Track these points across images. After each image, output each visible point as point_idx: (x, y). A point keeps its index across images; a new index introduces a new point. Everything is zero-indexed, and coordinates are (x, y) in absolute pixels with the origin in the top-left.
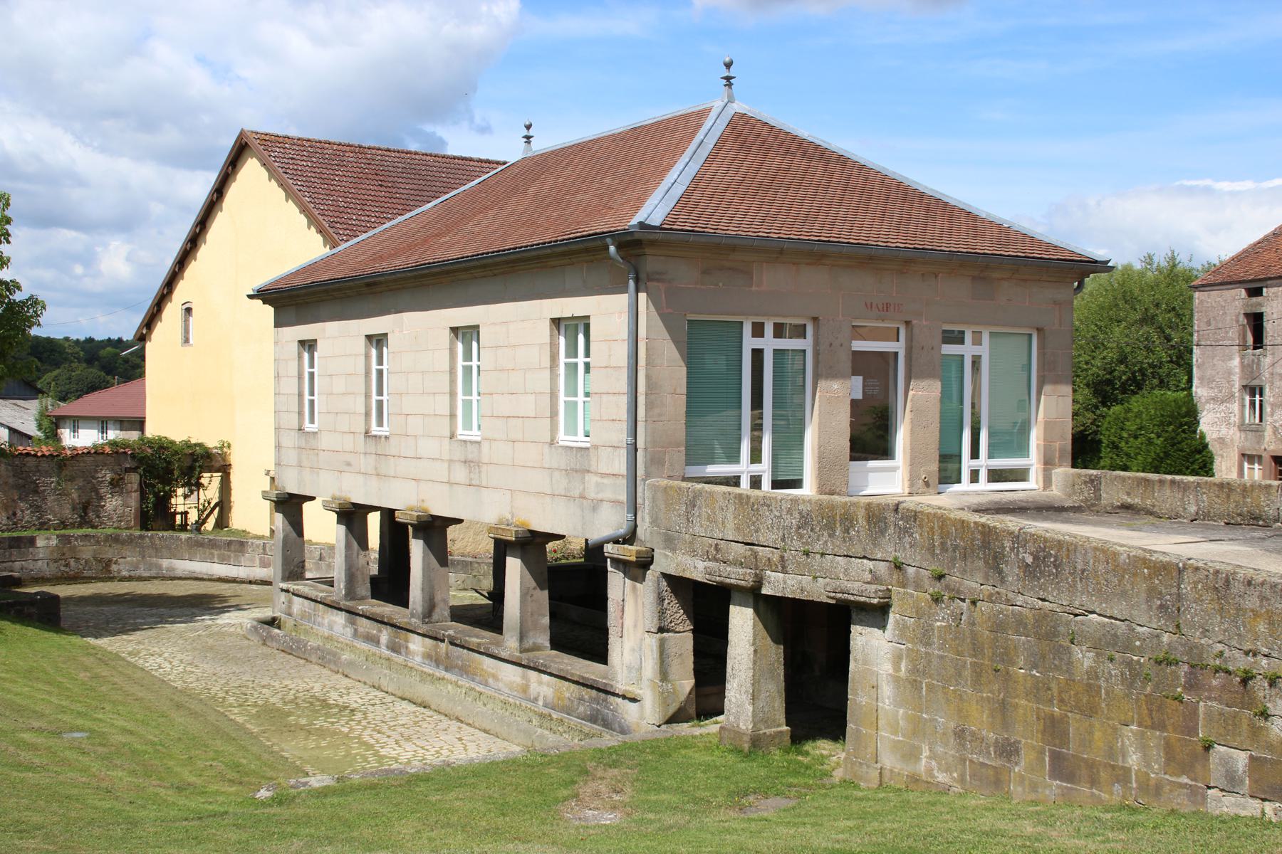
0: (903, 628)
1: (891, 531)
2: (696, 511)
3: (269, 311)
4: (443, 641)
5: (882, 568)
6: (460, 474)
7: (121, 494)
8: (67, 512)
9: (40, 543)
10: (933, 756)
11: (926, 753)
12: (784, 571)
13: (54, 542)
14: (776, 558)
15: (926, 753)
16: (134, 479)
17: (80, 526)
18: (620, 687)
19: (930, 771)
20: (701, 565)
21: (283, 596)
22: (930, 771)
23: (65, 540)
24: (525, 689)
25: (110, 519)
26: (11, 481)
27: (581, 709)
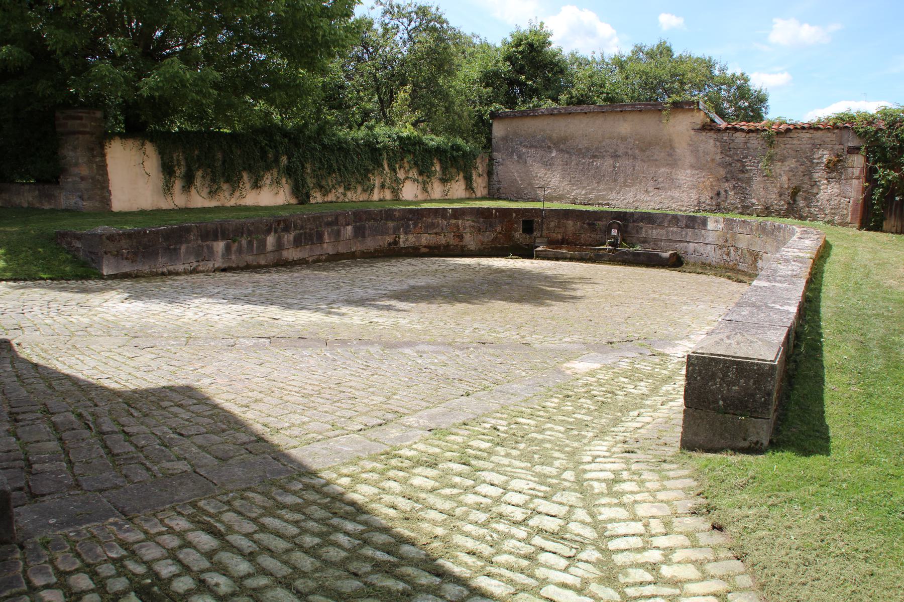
7: (839, 181)
8: (773, 197)
9: (711, 225)
13: (721, 226)
16: (857, 162)
17: (786, 215)
23: (730, 223)
25: (822, 210)
26: (718, 157)
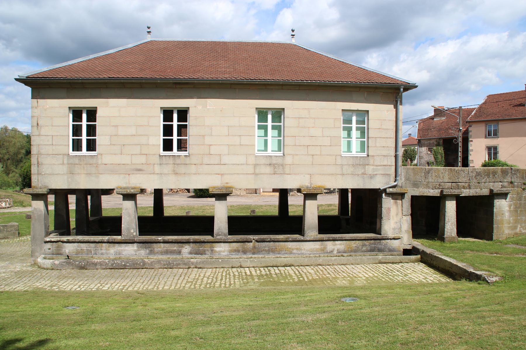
0: (512, 199)
1: (510, 174)
2: (430, 175)
3: (28, 90)
4: (251, 242)
5: (506, 184)
6: (268, 170)
10: (522, 227)
11: (519, 226)
12: (470, 188)
14: (467, 185)
15: (519, 226)
18: (391, 236)
19: (520, 231)
20: (432, 191)
21: (49, 245)
22: (520, 231)
24: (323, 250)
27: (364, 248)
